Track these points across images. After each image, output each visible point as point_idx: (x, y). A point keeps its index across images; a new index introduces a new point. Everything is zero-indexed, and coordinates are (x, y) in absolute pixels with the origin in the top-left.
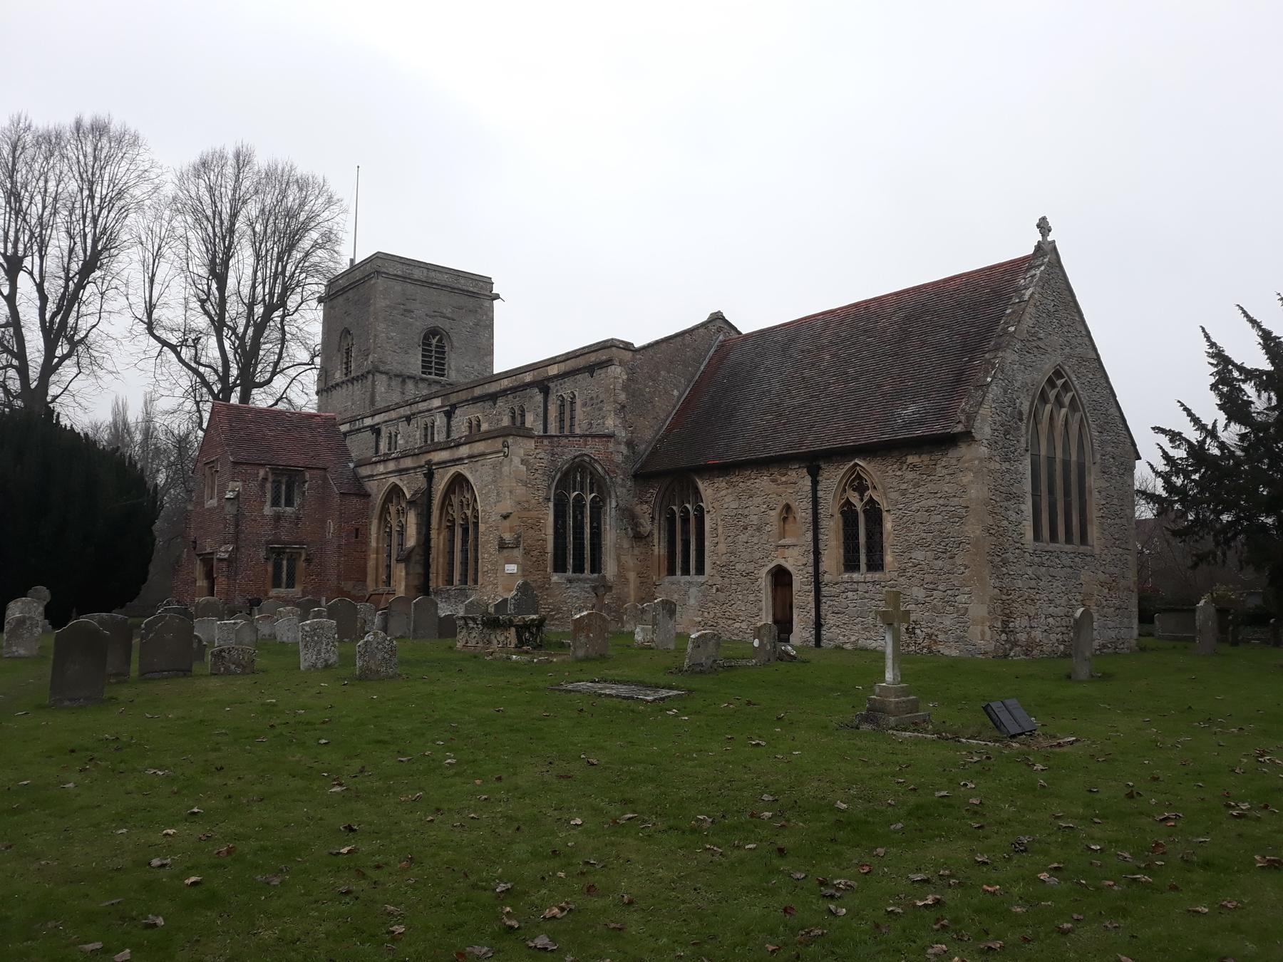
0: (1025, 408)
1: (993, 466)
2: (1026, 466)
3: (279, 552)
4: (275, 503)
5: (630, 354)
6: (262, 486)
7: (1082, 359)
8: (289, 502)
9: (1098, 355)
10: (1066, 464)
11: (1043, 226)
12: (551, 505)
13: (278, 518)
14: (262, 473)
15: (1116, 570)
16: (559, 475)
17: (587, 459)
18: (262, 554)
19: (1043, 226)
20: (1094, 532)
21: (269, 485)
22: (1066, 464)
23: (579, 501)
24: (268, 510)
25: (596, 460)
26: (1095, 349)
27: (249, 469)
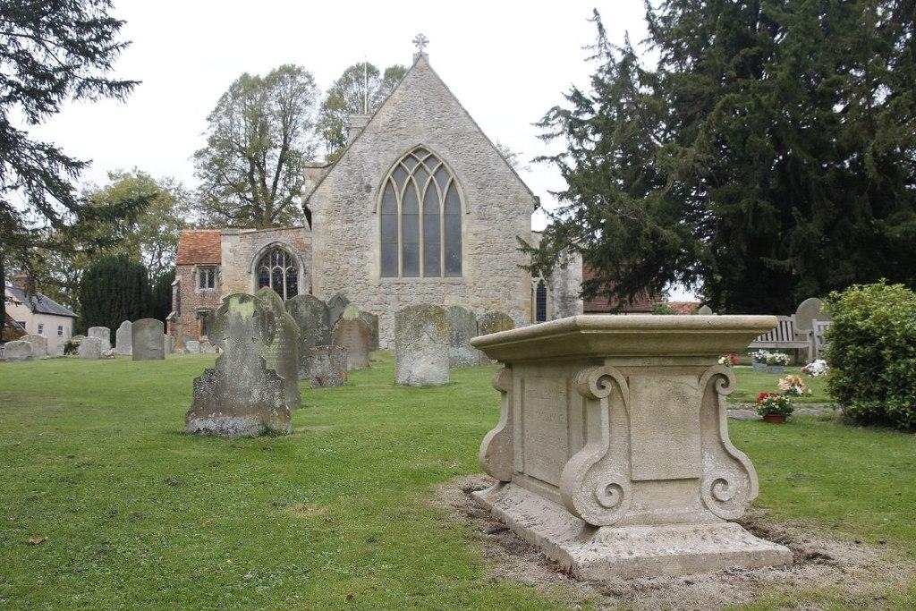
0: (375, 183)
1: (332, 227)
2: (374, 224)
3: (205, 314)
4: (202, 286)
5: (320, 170)
6: (194, 277)
7: (458, 135)
8: (211, 284)
9: (479, 128)
10: (431, 219)
11: (421, 41)
12: (253, 276)
13: (204, 294)
14: (193, 269)
15: (500, 295)
16: (257, 257)
17: (279, 244)
18: (195, 316)
19: (421, 41)
20: (466, 265)
21: (198, 276)
22: (431, 219)
23: (278, 272)
24: (198, 290)
25: (286, 245)
26: (476, 125)
27: (185, 267)
